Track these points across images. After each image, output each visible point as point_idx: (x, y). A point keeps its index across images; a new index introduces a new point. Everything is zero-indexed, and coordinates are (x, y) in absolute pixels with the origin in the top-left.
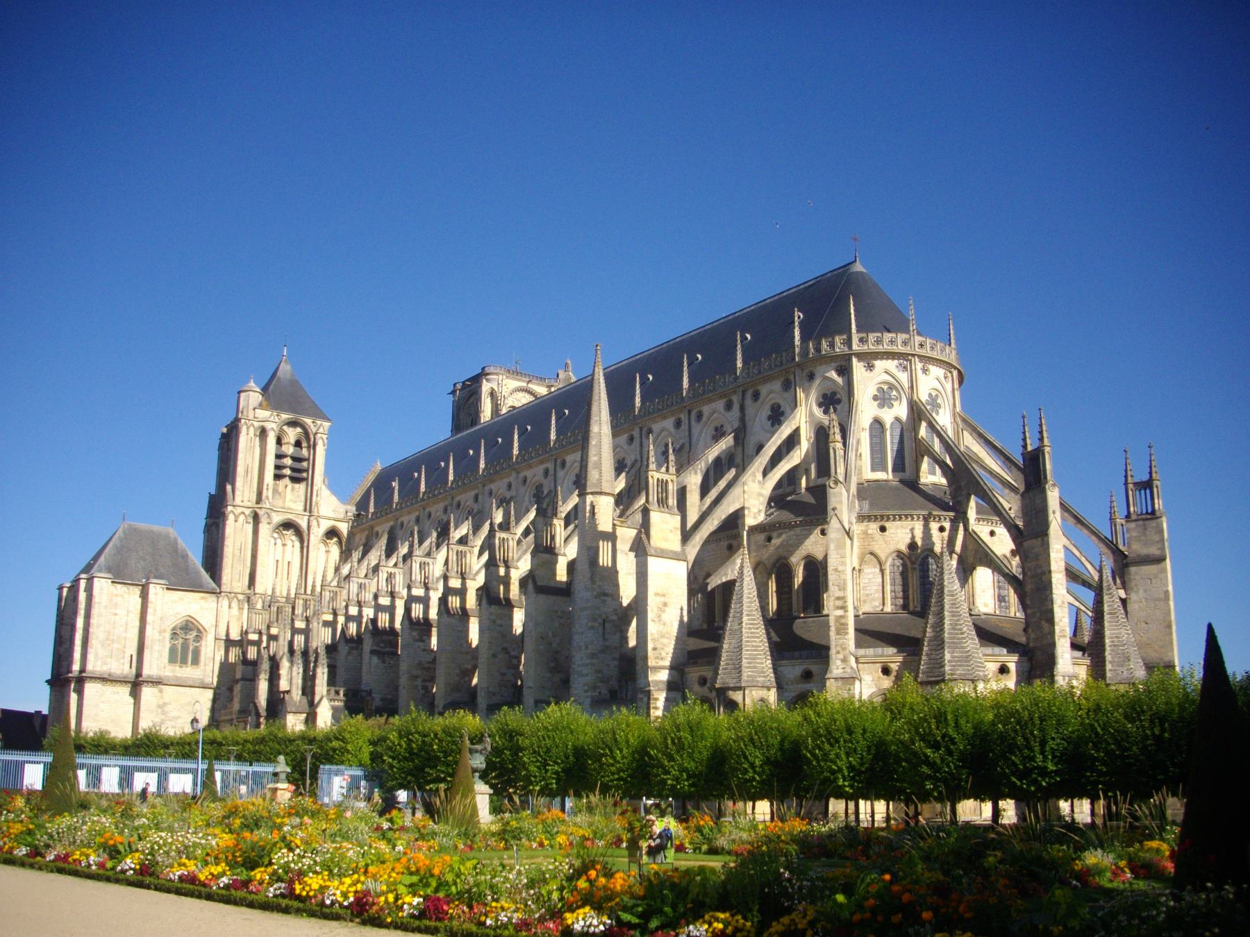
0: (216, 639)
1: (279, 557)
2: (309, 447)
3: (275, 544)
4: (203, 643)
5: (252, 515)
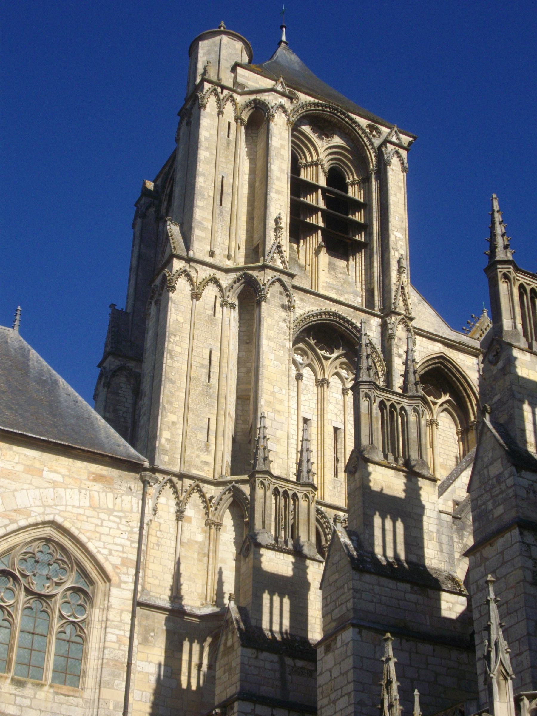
0: (137, 604)
1: (313, 417)
2: (365, 182)
3: (299, 377)
4: (97, 614)
5: (238, 288)
